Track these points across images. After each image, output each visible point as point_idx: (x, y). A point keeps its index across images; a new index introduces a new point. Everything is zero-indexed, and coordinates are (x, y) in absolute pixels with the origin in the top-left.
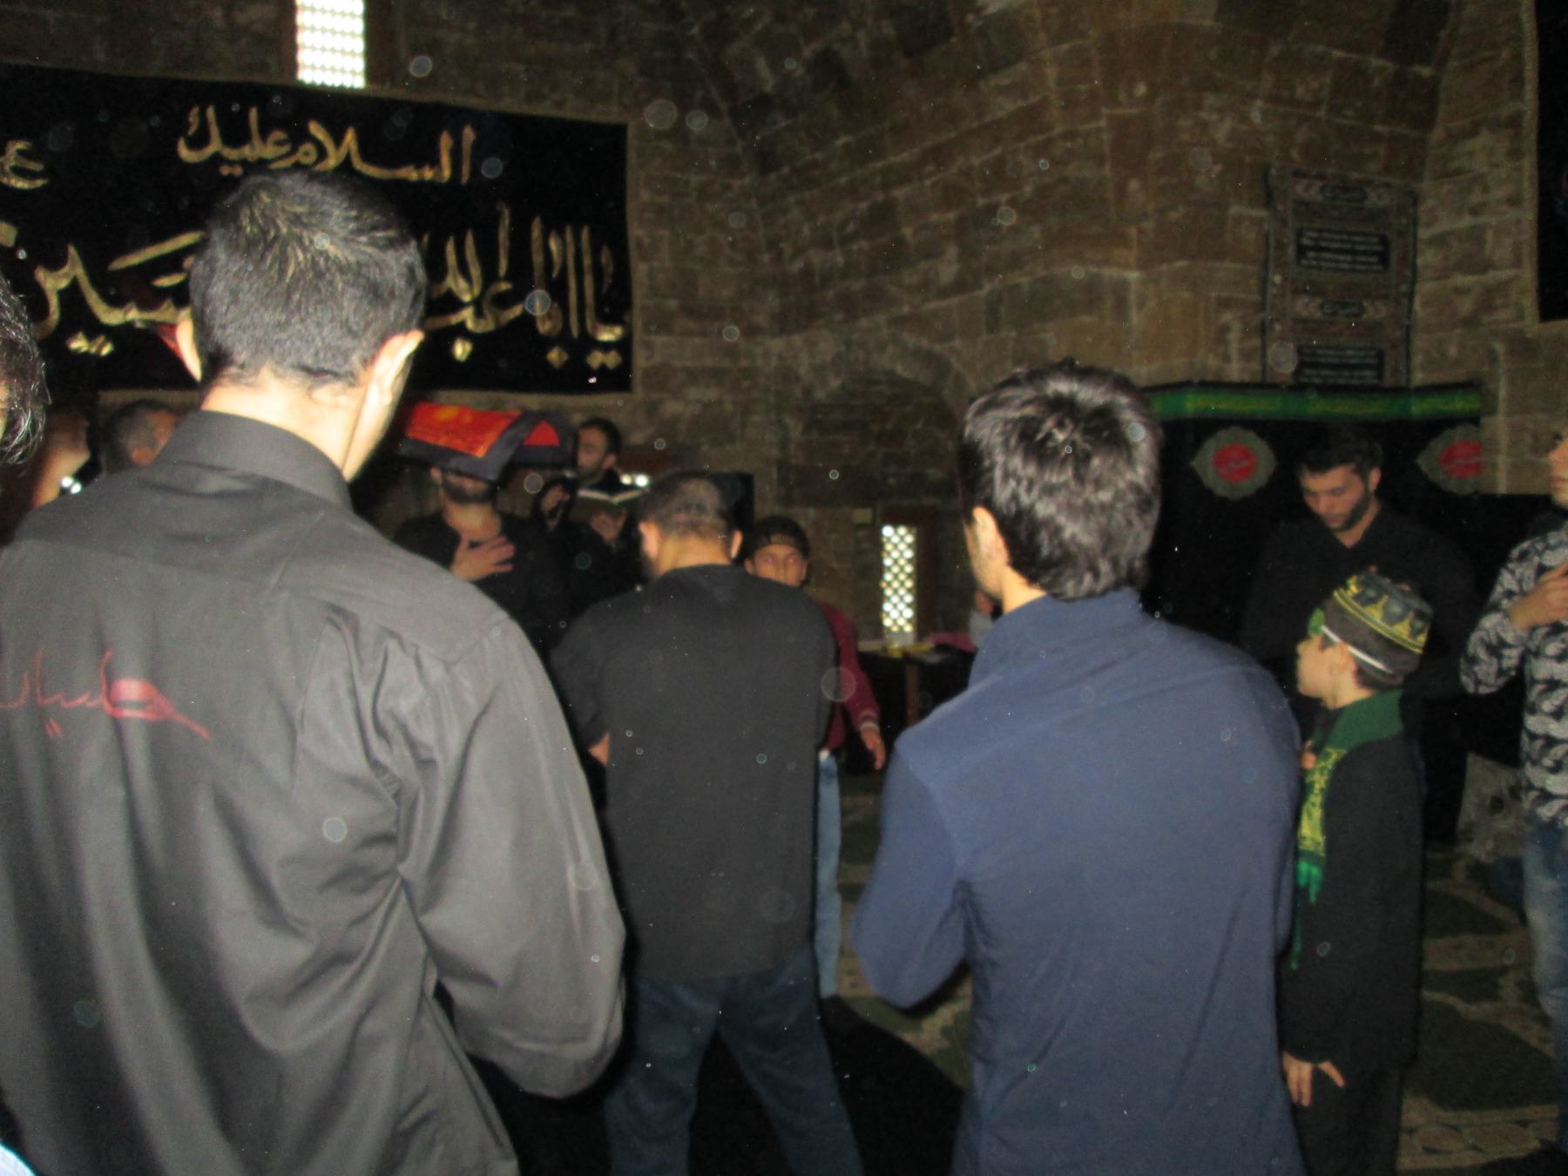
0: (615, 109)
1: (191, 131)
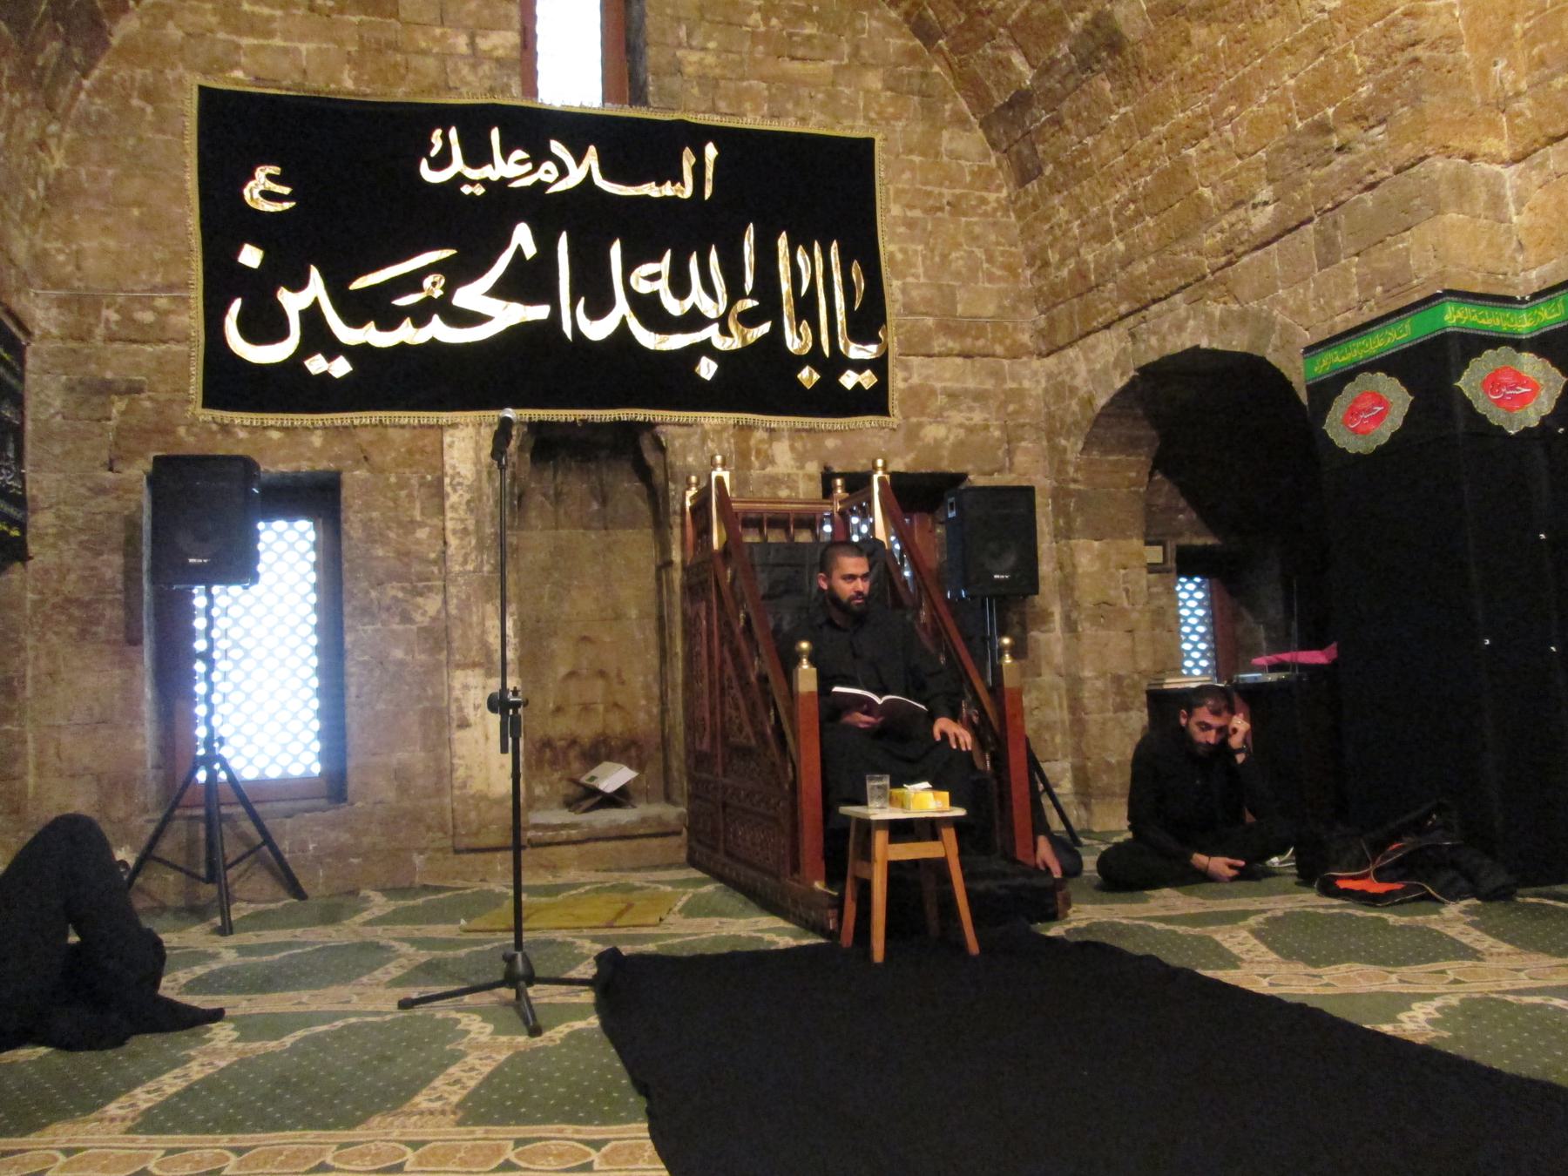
0: (861, 122)
1: (434, 153)
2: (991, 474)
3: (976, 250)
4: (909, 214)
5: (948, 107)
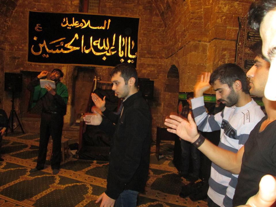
0: (137, 15)
3: (157, 39)
5: (154, 12)
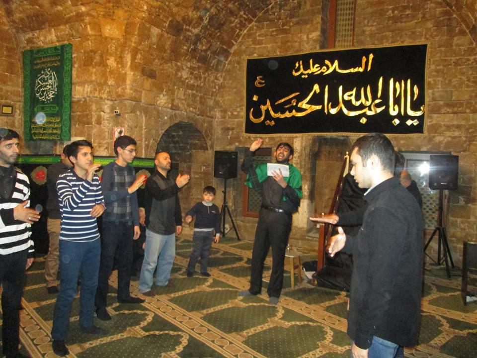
0: (423, 40)
2: (460, 152)
4: (438, 68)
